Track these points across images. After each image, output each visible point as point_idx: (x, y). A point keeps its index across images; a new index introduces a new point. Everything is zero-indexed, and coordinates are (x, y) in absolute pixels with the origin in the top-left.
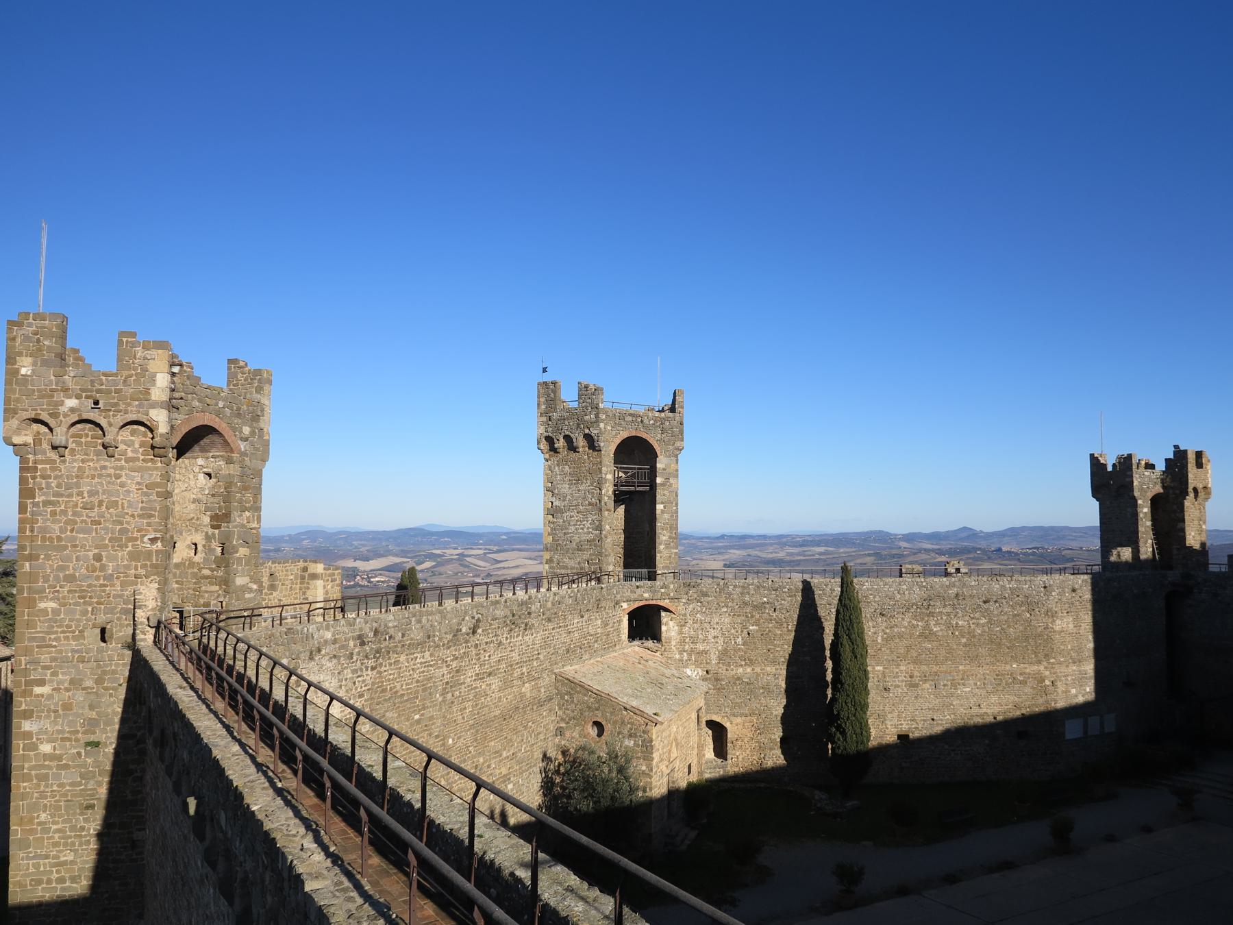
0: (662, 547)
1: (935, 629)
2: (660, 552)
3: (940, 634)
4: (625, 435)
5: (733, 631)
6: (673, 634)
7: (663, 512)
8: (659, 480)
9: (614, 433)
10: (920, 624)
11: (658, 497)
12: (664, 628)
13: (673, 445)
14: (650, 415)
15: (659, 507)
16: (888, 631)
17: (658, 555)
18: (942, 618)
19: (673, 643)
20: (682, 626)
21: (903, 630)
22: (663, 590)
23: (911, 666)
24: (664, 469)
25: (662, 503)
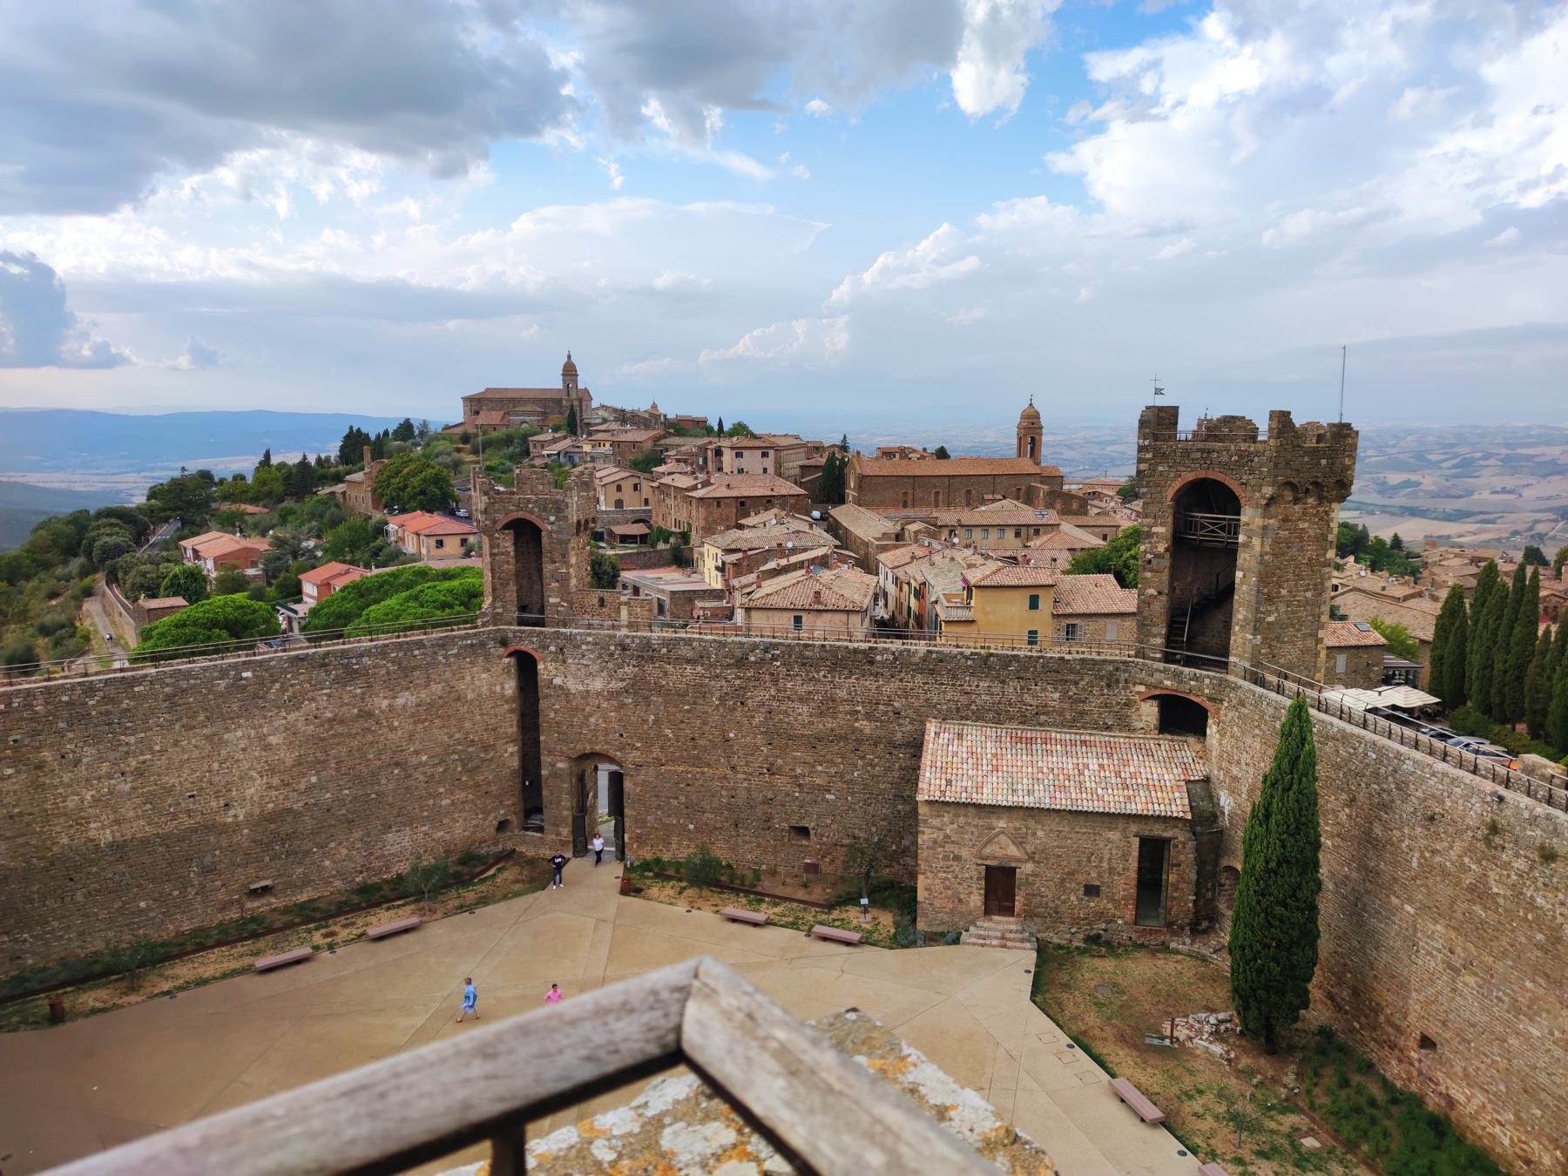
0: (1237, 628)
1: (1495, 890)
2: (1235, 635)
3: (1501, 901)
4: (1190, 476)
5: (1262, 765)
6: (1215, 742)
7: (1242, 582)
8: (1241, 538)
9: (1172, 475)
10: (1473, 867)
11: (1240, 562)
12: (1208, 731)
13: (1260, 491)
14: (1233, 448)
15: (1239, 574)
16: (1427, 855)
17: (1233, 638)
18: (1509, 876)
19: (1214, 753)
20: (1223, 736)
21: (1448, 864)
22: (1192, 683)
23: (1453, 935)
24: (1248, 524)
25: (1242, 570)
